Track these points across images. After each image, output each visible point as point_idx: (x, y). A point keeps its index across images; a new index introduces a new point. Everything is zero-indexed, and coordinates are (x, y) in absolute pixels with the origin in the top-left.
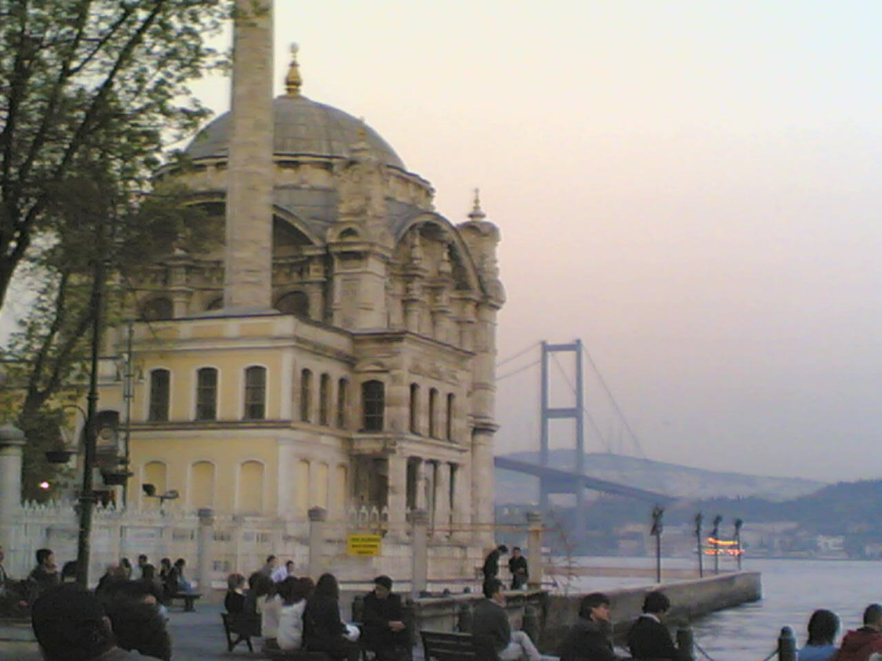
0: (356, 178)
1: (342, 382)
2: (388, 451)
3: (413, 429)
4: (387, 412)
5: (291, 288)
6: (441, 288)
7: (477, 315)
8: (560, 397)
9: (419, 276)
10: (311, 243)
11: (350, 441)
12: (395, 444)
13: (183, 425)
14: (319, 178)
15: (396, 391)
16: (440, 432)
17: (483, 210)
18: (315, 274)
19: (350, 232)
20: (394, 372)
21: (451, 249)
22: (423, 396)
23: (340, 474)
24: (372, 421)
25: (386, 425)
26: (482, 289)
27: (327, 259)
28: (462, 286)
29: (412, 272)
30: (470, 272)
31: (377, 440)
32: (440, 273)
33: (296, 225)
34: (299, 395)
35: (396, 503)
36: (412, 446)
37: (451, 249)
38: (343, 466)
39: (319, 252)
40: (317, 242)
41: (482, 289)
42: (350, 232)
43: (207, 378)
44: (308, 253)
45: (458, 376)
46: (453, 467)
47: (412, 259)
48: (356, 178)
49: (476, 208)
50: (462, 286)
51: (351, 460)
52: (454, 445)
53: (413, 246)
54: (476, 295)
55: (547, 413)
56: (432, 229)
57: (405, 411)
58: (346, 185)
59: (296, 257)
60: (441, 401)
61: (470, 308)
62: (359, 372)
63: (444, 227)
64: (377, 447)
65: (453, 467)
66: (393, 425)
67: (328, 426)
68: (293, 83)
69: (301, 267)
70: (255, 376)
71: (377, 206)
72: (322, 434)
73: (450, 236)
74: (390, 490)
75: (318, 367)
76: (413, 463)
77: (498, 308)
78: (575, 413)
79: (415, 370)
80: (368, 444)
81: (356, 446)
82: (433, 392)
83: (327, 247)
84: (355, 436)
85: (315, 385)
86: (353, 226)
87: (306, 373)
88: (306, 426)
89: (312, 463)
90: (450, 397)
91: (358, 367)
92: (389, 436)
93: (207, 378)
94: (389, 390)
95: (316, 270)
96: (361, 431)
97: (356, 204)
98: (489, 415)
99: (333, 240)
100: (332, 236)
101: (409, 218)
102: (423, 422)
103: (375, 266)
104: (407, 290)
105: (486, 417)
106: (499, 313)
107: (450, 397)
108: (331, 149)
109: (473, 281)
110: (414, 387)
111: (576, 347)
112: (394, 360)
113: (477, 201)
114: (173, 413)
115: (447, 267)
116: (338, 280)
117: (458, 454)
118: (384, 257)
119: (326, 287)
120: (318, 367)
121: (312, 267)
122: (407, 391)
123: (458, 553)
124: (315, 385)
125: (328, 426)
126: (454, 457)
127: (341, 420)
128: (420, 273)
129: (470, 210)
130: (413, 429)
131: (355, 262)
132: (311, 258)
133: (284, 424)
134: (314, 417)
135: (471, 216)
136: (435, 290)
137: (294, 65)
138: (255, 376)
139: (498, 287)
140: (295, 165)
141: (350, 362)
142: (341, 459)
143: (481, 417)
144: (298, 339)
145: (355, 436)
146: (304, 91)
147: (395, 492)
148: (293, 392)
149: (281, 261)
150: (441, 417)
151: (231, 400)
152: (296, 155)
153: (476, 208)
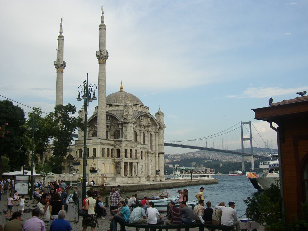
1: (112, 149)
3: (126, 156)
4: (121, 154)
5: (117, 129)
7: (159, 131)
8: (246, 136)
14: (121, 108)
15: (122, 151)
18: (120, 127)
19: (125, 119)
21: (151, 119)
22: (128, 151)
23: (113, 165)
24: (118, 156)
27: (122, 124)
28: (156, 125)
30: (157, 123)
36: (125, 160)
38: (113, 164)
40: (120, 121)
41: (160, 126)
42: (125, 119)
44: (118, 123)
45: (138, 146)
46: (138, 163)
47: (141, 122)
54: (158, 127)
55: (243, 139)
56: (147, 116)
57: (124, 154)
60: (133, 152)
61: (157, 130)
63: (149, 115)
64: (119, 160)
65: (138, 163)
67: (109, 157)
68: (121, 89)
69: (118, 125)
70: (95, 149)
71: (131, 112)
75: (106, 147)
76: (126, 163)
78: (250, 139)
79: (126, 146)
80: (117, 160)
82: (131, 150)
83: (122, 122)
85: (106, 150)
87: (104, 149)
88: (104, 158)
90: (136, 150)
94: (121, 150)
96: (116, 158)
98: (162, 150)
99: (122, 120)
101: (139, 115)
102: (128, 155)
103: (130, 125)
107: (136, 150)
109: (158, 124)
110: (126, 150)
113: (159, 108)
115: (150, 123)
116: (124, 128)
117: (138, 161)
118: (132, 123)
119: (122, 129)
120: (106, 147)
121: (120, 125)
122: (124, 150)
123: (138, 178)
124: (106, 150)
126: (137, 161)
127: (112, 156)
130: (126, 156)
131: (127, 124)
132: (119, 124)
133: (99, 158)
134: (106, 156)
136: (148, 127)
138: (95, 149)
139: (164, 125)
140: (118, 106)
141: (114, 146)
144: (100, 143)
146: (124, 90)
147: (122, 168)
148: (100, 152)
150: (133, 154)
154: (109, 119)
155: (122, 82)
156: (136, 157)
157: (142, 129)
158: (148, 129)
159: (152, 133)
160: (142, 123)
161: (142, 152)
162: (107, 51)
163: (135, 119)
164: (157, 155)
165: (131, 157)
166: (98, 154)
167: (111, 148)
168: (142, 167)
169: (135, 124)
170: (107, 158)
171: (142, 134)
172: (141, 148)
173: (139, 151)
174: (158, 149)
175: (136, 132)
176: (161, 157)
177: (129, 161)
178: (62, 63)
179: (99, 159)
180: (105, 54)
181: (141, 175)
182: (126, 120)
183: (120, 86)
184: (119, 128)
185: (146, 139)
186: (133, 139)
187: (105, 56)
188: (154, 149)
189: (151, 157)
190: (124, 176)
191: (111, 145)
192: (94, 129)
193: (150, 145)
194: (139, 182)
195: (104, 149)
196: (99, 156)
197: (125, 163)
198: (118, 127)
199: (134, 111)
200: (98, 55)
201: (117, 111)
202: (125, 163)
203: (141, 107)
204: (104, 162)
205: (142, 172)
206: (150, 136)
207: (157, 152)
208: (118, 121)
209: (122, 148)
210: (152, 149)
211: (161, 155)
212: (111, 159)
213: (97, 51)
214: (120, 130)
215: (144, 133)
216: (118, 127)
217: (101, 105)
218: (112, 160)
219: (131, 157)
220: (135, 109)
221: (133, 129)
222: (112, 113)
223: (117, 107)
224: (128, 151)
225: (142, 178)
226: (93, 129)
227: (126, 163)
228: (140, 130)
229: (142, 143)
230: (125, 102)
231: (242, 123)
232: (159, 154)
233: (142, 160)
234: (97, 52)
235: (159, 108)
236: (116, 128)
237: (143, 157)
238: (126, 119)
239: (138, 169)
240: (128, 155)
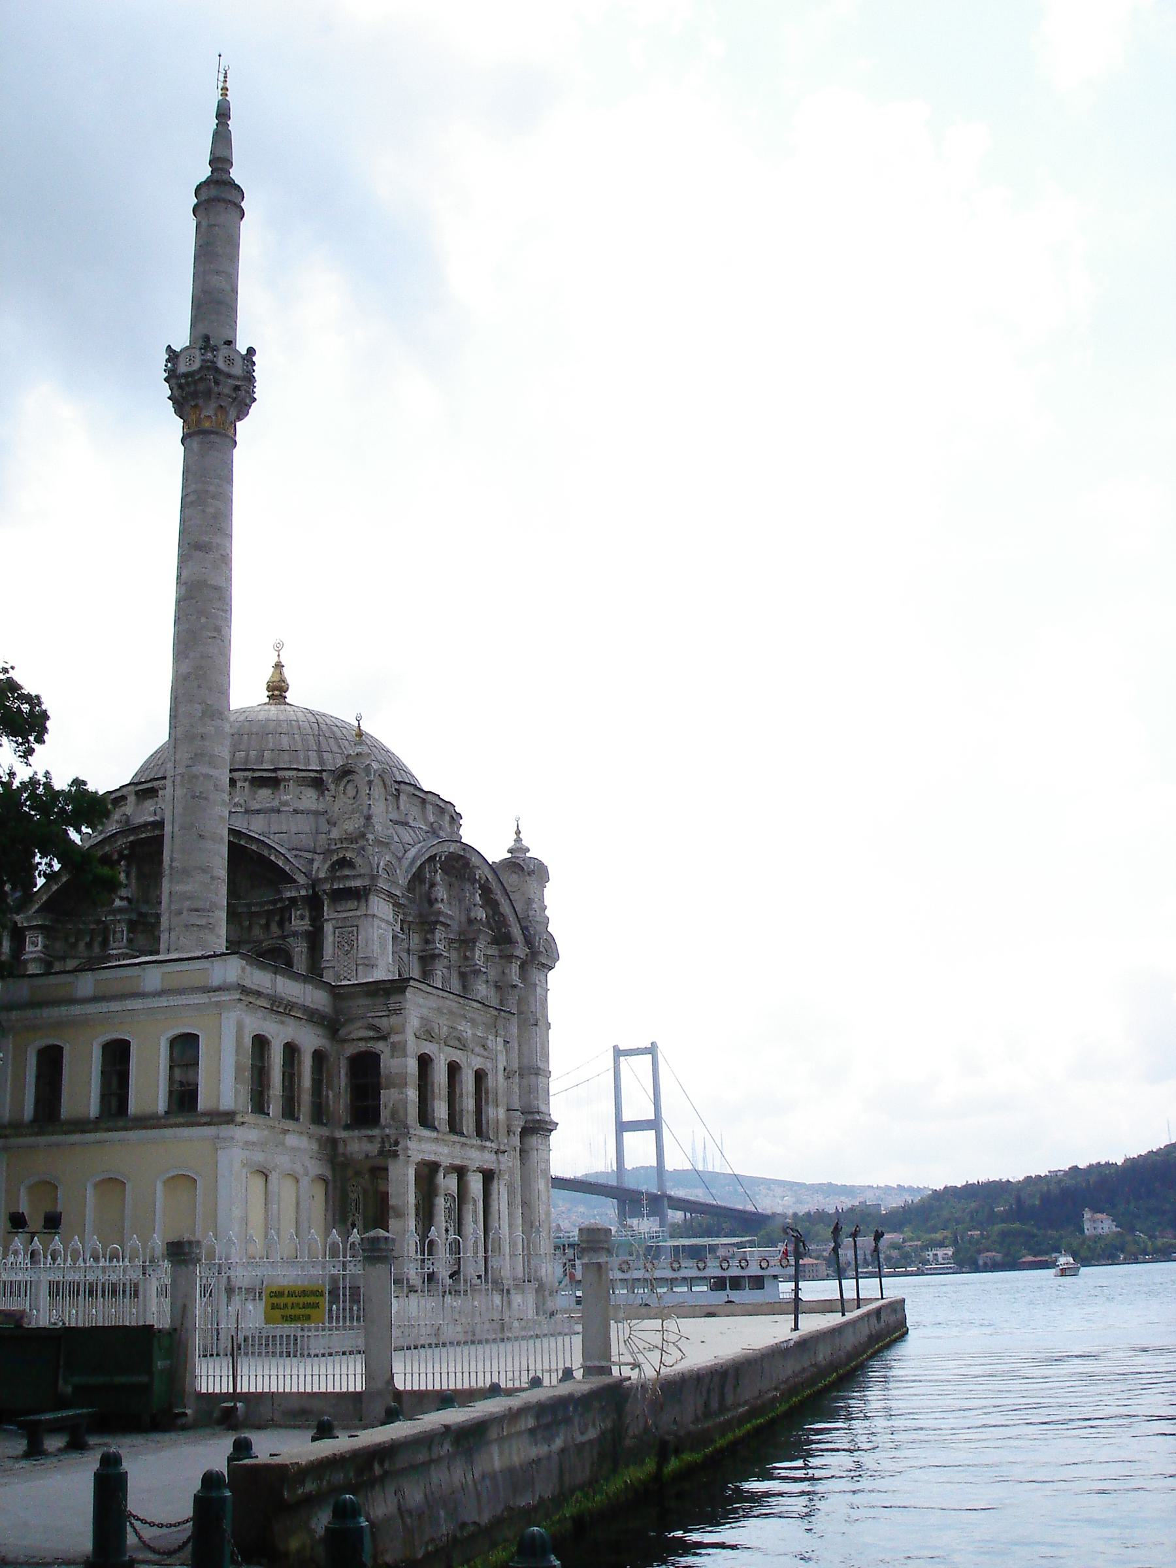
0: (351, 792)
1: (319, 1057)
2: (389, 1151)
3: (425, 1120)
4: (388, 1097)
6: (474, 941)
8: (637, 1108)
9: (443, 924)
10: (295, 881)
11: (333, 1142)
12: (397, 1143)
13: (81, 1125)
16: (468, 1125)
17: (526, 843)
18: (299, 923)
19: (344, 863)
20: (394, 1038)
21: (486, 890)
22: (440, 1076)
23: (319, 1191)
25: (385, 1114)
26: (528, 942)
27: (314, 903)
28: (502, 939)
29: (433, 918)
30: (511, 918)
31: (371, 1138)
32: (471, 921)
33: (273, 858)
34: (247, 1074)
35: (404, 1230)
36: (426, 1146)
37: (486, 890)
38: (322, 1178)
39: (303, 893)
40: (302, 880)
41: (528, 942)
44: (288, 894)
46: (488, 1177)
48: (351, 792)
49: (518, 840)
50: (502, 939)
51: (333, 1169)
52: (488, 1144)
53: (433, 885)
54: (521, 951)
55: (622, 1127)
57: (412, 1094)
58: (339, 802)
59: (274, 902)
61: (515, 968)
62: (344, 1041)
63: (474, 860)
64: (373, 1148)
65: (488, 1177)
66: (394, 1114)
67: (297, 1119)
68: (277, 690)
72: (286, 1132)
73: (482, 873)
74: (391, 1213)
75: (279, 1033)
76: (428, 1173)
77: (551, 968)
78: (654, 1125)
79: (428, 1035)
81: (341, 1149)
82: (453, 1069)
83: (315, 883)
84: (341, 1134)
86: (348, 855)
87: (261, 1043)
89: (273, 1177)
90: (480, 1076)
91: (342, 1032)
92: (387, 1131)
94: (389, 1064)
95: (302, 918)
96: (347, 1127)
97: (351, 825)
98: (543, 1108)
99: (322, 875)
100: (320, 868)
102: (441, 1110)
103: (381, 908)
104: (427, 942)
105: (538, 1112)
106: (551, 974)
107: (480, 1076)
108: (322, 761)
109: (516, 932)
110: (425, 1062)
111: (652, 1050)
112: (394, 1020)
113: (518, 832)
114: (68, 1108)
115: (481, 914)
116: (328, 928)
117: (494, 1156)
119: (315, 939)
120: (279, 1033)
121: (295, 914)
122: (412, 1065)
125: (297, 1119)
128: (442, 919)
129: (511, 843)
131: (352, 904)
132: (290, 899)
133: (227, 1118)
134: (275, 1107)
135: (510, 851)
136: (465, 942)
137: (279, 666)
141: (331, 1025)
142: (316, 1168)
143: (533, 1113)
144: (244, 990)
145: (341, 1134)
146: (290, 697)
148: (239, 1068)
149: (253, 909)
150: (468, 1103)
152: (275, 770)
153: (518, 840)
155: (278, 648)
158: (466, 958)
162: (251, 351)
165: (454, 1126)
170: (289, 1124)
179: (225, 1131)
180: (237, 370)
182: (347, 872)
183: (267, 674)
184: (295, 934)
191: (313, 1017)
192: (89, 946)
195: (261, 1043)
196: (227, 1102)
198: (274, 928)
200: (186, 375)
201: (274, 816)
204: (259, 1157)
208: (289, 879)
209: (399, 1049)
211: (534, 1140)
213: (177, 348)
216: (274, 928)
217: (201, 730)
218: (315, 1147)
219: (454, 1126)
221: (394, 937)
223: (265, 793)
224: (440, 1076)
226: (82, 946)
227: (428, 1173)
230: (322, 761)
231: (618, 1053)
234: (173, 356)
235: (518, 832)
236: (257, 932)
238: (350, 864)
240: (441, 1110)
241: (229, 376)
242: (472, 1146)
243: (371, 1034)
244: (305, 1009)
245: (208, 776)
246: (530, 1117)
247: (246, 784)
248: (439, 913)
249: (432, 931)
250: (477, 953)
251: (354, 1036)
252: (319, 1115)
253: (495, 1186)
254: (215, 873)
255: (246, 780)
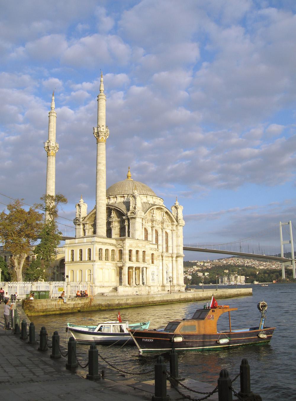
1: (113, 251)
4: (124, 257)
13: (77, 262)
15: (126, 252)
22: (134, 253)
27: (128, 219)
41: (177, 222)
43: (81, 251)
45: (146, 247)
57: (127, 257)
60: (141, 254)
61: (175, 226)
63: (163, 208)
65: (146, 268)
67: (108, 260)
72: (106, 263)
75: (104, 248)
79: (131, 246)
81: (117, 265)
82: (137, 252)
85: (104, 252)
87: (100, 250)
90: (144, 252)
93: (81, 251)
94: (124, 252)
96: (118, 261)
101: (150, 207)
102: (134, 258)
110: (130, 251)
116: (130, 224)
117: (147, 265)
118: (141, 218)
123: (147, 288)
124: (104, 252)
127: (113, 259)
130: (130, 260)
131: (134, 220)
133: (94, 261)
134: (104, 258)
136: (162, 223)
148: (96, 254)
151: (85, 257)
154: (112, 213)
156: (144, 261)
157: (154, 225)
159: (168, 231)
160: (154, 217)
161: (153, 254)
163: (145, 213)
164: (174, 259)
166: (95, 256)
167: (111, 248)
168: (153, 274)
169: (144, 219)
171: (154, 232)
172: (151, 249)
173: (149, 253)
174: (175, 251)
175: (146, 230)
176: (179, 261)
177: (134, 265)
178: (54, 145)
181: (152, 284)
185: (160, 238)
186: (143, 237)
187: (105, 134)
188: (170, 251)
189: (167, 261)
190: (128, 285)
193: (165, 246)
194: (149, 292)
195: (100, 250)
197: (129, 268)
199: (144, 203)
202: (129, 268)
203: (153, 198)
205: (153, 280)
206: (164, 234)
207: (175, 256)
210: (167, 251)
211: (179, 259)
212: (111, 263)
214: (127, 227)
215: (157, 232)
218: (112, 264)
219: (137, 261)
220: (145, 200)
222: (116, 205)
225: (152, 288)
228: (152, 227)
229: (154, 243)
232: (177, 257)
233: (152, 264)
237: (155, 261)
239: (147, 276)
241: (103, 132)
242: (141, 264)
243: (121, 247)
244: (109, 243)
245: (102, 203)
246: (178, 254)
247: (119, 197)
248: (154, 219)
249: (153, 222)
250: (164, 225)
251: (119, 247)
252: (113, 259)
253: (147, 270)
254: (103, 219)
255: (118, 197)
